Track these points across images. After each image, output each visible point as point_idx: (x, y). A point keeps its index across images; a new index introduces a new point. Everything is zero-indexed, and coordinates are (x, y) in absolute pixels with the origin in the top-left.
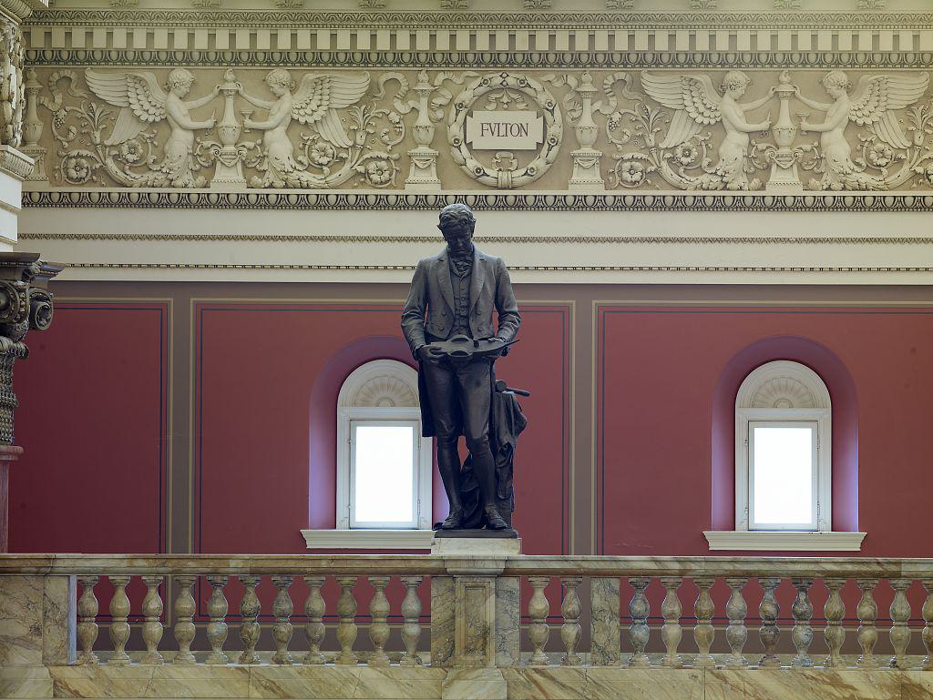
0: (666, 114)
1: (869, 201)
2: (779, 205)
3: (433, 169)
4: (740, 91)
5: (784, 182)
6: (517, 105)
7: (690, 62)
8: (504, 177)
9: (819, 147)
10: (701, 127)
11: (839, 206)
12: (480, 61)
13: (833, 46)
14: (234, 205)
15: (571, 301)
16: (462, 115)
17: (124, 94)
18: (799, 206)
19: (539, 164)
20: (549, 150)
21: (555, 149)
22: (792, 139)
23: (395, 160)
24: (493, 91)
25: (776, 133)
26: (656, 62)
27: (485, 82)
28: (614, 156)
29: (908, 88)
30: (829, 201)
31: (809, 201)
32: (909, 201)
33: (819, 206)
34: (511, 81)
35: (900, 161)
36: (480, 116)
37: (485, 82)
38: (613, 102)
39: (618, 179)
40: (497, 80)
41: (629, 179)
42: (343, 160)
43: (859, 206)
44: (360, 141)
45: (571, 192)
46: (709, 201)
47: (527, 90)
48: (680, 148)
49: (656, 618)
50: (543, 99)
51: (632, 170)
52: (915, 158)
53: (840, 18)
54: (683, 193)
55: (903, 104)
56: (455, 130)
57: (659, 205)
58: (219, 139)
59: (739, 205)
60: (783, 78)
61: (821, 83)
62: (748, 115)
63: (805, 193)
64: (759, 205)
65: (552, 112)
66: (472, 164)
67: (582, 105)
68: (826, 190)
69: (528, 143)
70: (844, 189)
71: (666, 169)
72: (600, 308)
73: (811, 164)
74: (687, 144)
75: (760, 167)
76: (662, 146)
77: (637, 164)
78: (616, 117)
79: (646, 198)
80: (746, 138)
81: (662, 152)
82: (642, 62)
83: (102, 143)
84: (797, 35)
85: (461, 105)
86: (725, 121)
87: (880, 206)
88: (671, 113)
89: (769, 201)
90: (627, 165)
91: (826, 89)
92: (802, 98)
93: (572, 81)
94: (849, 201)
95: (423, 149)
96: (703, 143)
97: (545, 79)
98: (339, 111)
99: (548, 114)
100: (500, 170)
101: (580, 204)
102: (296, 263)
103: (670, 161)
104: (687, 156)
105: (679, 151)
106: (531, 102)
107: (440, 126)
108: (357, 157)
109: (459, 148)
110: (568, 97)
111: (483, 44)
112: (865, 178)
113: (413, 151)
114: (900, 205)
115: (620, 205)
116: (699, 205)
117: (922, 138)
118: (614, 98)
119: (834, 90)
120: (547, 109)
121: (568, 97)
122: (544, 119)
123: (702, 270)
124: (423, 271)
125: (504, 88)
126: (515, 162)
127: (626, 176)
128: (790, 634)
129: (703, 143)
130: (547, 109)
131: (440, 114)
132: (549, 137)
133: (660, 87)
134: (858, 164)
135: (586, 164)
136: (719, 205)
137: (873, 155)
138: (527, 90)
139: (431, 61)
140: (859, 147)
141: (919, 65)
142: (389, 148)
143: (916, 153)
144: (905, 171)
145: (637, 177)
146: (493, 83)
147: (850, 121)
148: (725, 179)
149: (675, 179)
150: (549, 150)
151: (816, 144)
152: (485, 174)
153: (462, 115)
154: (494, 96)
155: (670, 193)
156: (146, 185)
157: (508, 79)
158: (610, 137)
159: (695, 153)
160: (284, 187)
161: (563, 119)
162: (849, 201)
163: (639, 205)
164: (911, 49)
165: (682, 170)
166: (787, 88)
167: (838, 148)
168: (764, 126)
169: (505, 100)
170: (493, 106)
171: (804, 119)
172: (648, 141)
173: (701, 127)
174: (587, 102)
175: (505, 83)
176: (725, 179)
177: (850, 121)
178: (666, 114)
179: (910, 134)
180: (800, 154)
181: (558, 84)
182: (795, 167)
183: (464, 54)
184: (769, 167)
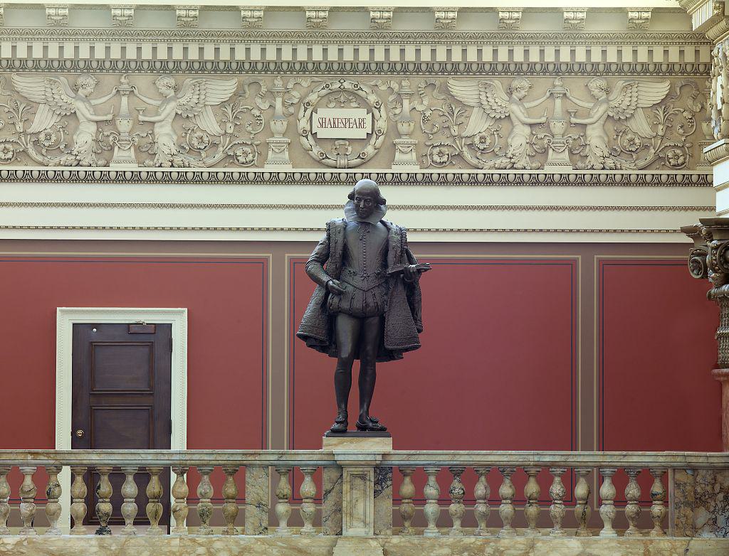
0: (31, 106)
1: (190, 176)
2: (121, 178)
3: (287, 153)
4: (89, 90)
5: (124, 161)
6: (352, 104)
7: (50, 68)
8: (343, 162)
9: (585, 136)
10: (60, 117)
11: (167, 179)
12: (327, 68)
13: (556, 58)
14: (67, 180)
15: (269, 255)
16: (308, 112)
17: (43, 93)
18: (136, 179)
19: (370, 150)
20: (377, 139)
21: (381, 138)
22: (131, 126)
23: (257, 146)
24: (332, 92)
25: (118, 122)
26: (22, 67)
27: (327, 86)
28: (427, 143)
29: (656, 91)
30: (159, 175)
31: (144, 175)
32: (312, 177)
33: (152, 179)
34: (347, 85)
35: (215, 145)
36: (323, 113)
37: (327, 86)
38: (425, 102)
39: (430, 160)
40: (336, 86)
41: (438, 161)
42: (215, 145)
43: (182, 180)
44: (230, 131)
45: (268, 168)
46: (67, 175)
47: (360, 92)
48: (477, 136)
49: (420, 499)
50: (372, 99)
51: (441, 154)
52: (226, 145)
53: (161, 33)
54: (46, 168)
55: (216, 101)
56: (303, 124)
57: (459, 181)
58: (117, 129)
59: (89, 179)
60: (123, 80)
61: (154, 83)
62: (96, 110)
63: (140, 169)
64: (105, 179)
65: (379, 109)
66: (315, 152)
67: (402, 104)
68: (159, 167)
69: (361, 134)
70: (172, 166)
71: (32, 152)
72: (291, 259)
73: (146, 150)
74: (49, 130)
75: (104, 148)
76: (30, 131)
77: (443, 149)
78: (428, 114)
79: (325, 175)
80: (93, 128)
81: (464, 139)
82: (443, 71)
83: (24, 133)
84: (156, 48)
85: (308, 104)
86: (77, 112)
87: (198, 179)
88: (34, 105)
89: (113, 175)
90: (438, 149)
91: (590, 91)
92: (138, 95)
93: (395, 86)
94: (174, 176)
95: (278, 138)
96: (61, 130)
97: (372, 83)
98: (213, 107)
99: (376, 112)
100: (339, 154)
101: (275, 180)
102: (137, 225)
103: (470, 146)
104: (482, 143)
105: (42, 137)
106: (363, 102)
107: (292, 118)
108: (227, 142)
109: (307, 137)
110: (391, 98)
111: (271, 55)
112: (191, 159)
113: (270, 139)
114: (213, 180)
115: (428, 181)
116: (58, 178)
117: (232, 128)
118: (427, 98)
119: (163, 90)
120: (375, 107)
121: (391, 98)
122: (373, 114)
123: (256, 230)
124: (330, 228)
125: (344, 90)
126: (350, 149)
127: (436, 158)
128: (549, 512)
129: (61, 130)
130: (375, 107)
131: (292, 110)
132: (375, 127)
133: (463, 89)
134: (183, 148)
135: (406, 149)
136: (74, 179)
137: (195, 142)
138: (360, 92)
139: (278, 68)
140: (184, 135)
141: (405, 72)
142: (252, 136)
143: (228, 139)
144: (219, 156)
145: (10, 155)
146: (333, 87)
147: (177, 114)
148: (78, 158)
149: (40, 158)
150: (377, 139)
151: (150, 132)
152: (327, 157)
153: (308, 112)
154: (332, 98)
155: (36, 168)
156: (60, 165)
157: (344, 84)
158: (423, 127)
159: (53, 138)
160: (171, 167)
161: (388, 118)
162: (174, 176)
163: (443, 181)
164: (538, 60)
165: (44, 151)
166: (558, 89)
167: (166, 138)
168: (109, 117)
169: (342, 99)
170: (332, 105)
171: (141, 112)
172: (18, 128)
173: (60, 117)
174: (406, 102)
175: (342, 87)
176: (78, 158)
177: (177, 114)
178: (31, 106)
179: (222, 124)
180: (136, 139)
181: (383, 88)
182: (132, 149)
183: (177, 63)
184: (112, 149)
